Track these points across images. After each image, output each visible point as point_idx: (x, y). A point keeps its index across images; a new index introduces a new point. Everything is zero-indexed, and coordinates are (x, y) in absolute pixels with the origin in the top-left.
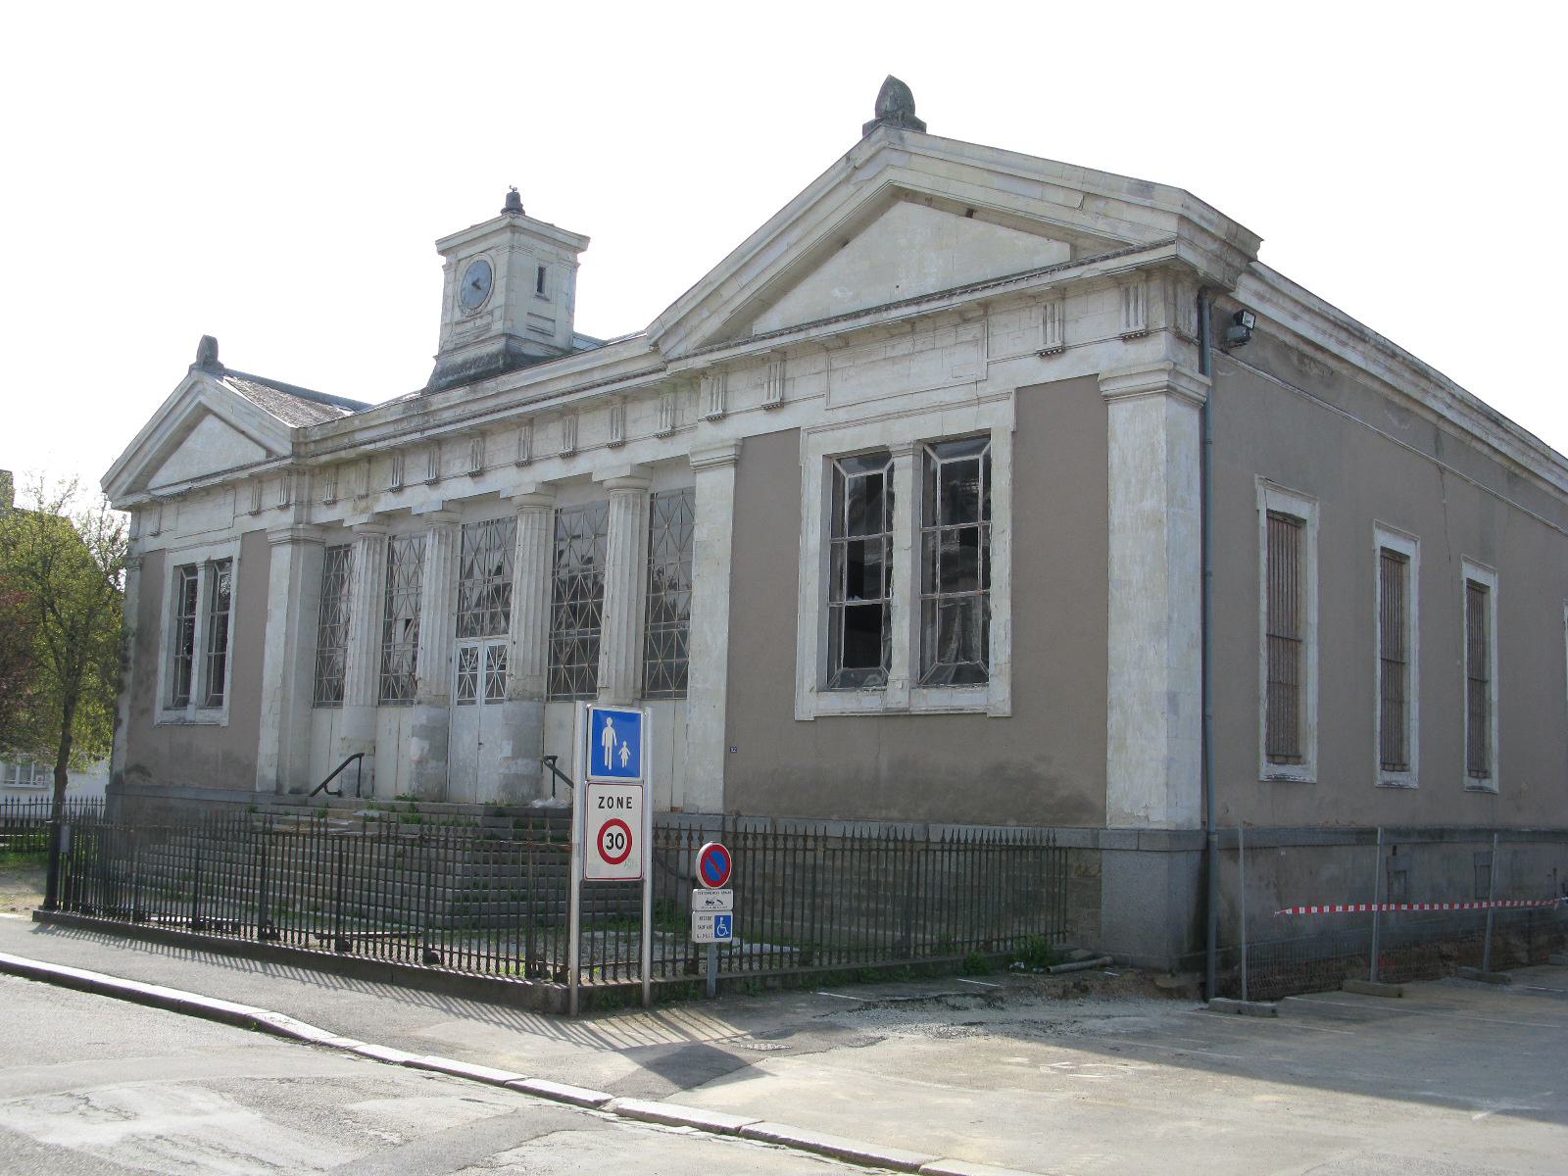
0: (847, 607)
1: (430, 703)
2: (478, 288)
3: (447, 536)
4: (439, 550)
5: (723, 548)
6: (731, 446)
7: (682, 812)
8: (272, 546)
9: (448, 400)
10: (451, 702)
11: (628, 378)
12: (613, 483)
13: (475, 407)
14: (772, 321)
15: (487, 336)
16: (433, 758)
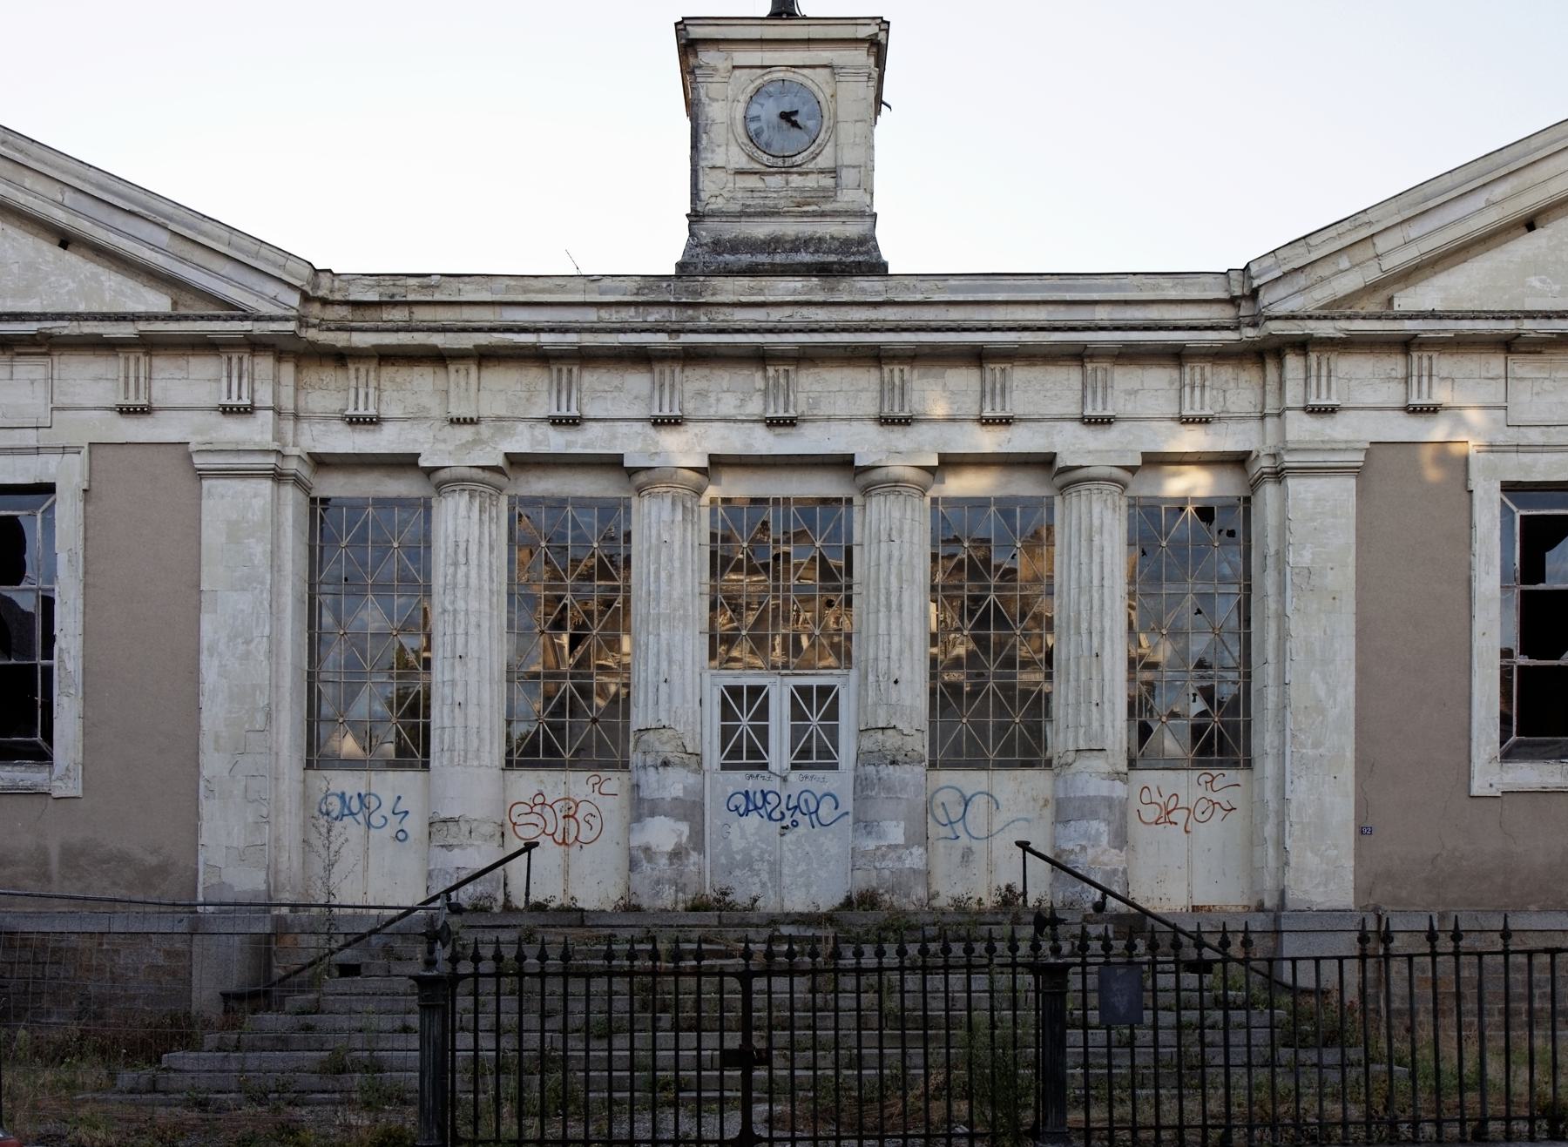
0: (1521, 668)
1: (684, 765)
2: (795, 124)
3: (693, 511)
4: (685, 530)
5: (1342, 578)
6: (1361, 450)
7: (1210, 910)
8: (201, 475)
9: (761, 291)
10: (706, 766)
11: (1161, 328)
12: (1105, 472)
13: (820, 315)
14: (1406, 300)
15: (827, 207)
16: (694, 849)
